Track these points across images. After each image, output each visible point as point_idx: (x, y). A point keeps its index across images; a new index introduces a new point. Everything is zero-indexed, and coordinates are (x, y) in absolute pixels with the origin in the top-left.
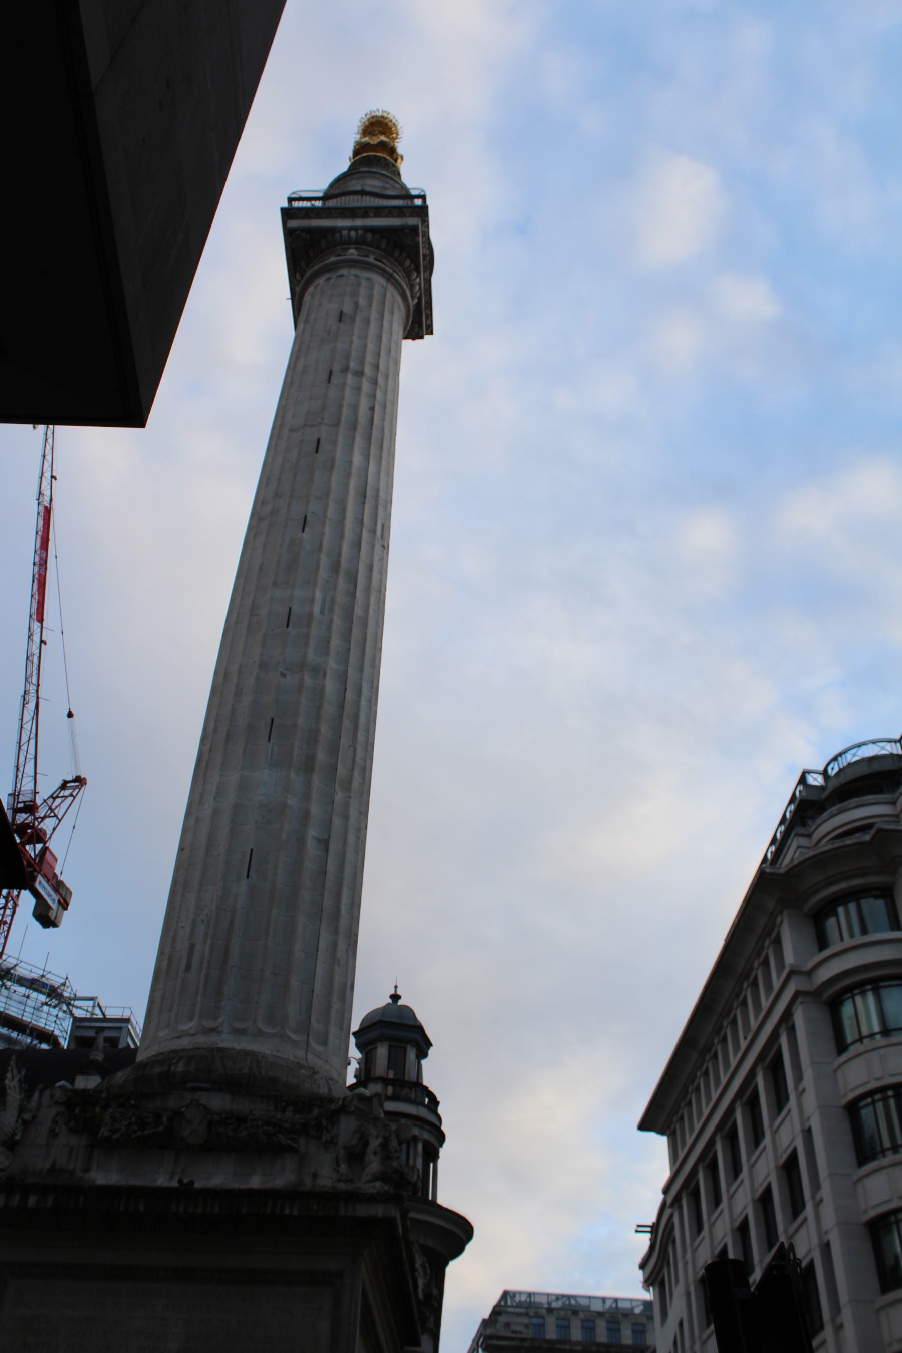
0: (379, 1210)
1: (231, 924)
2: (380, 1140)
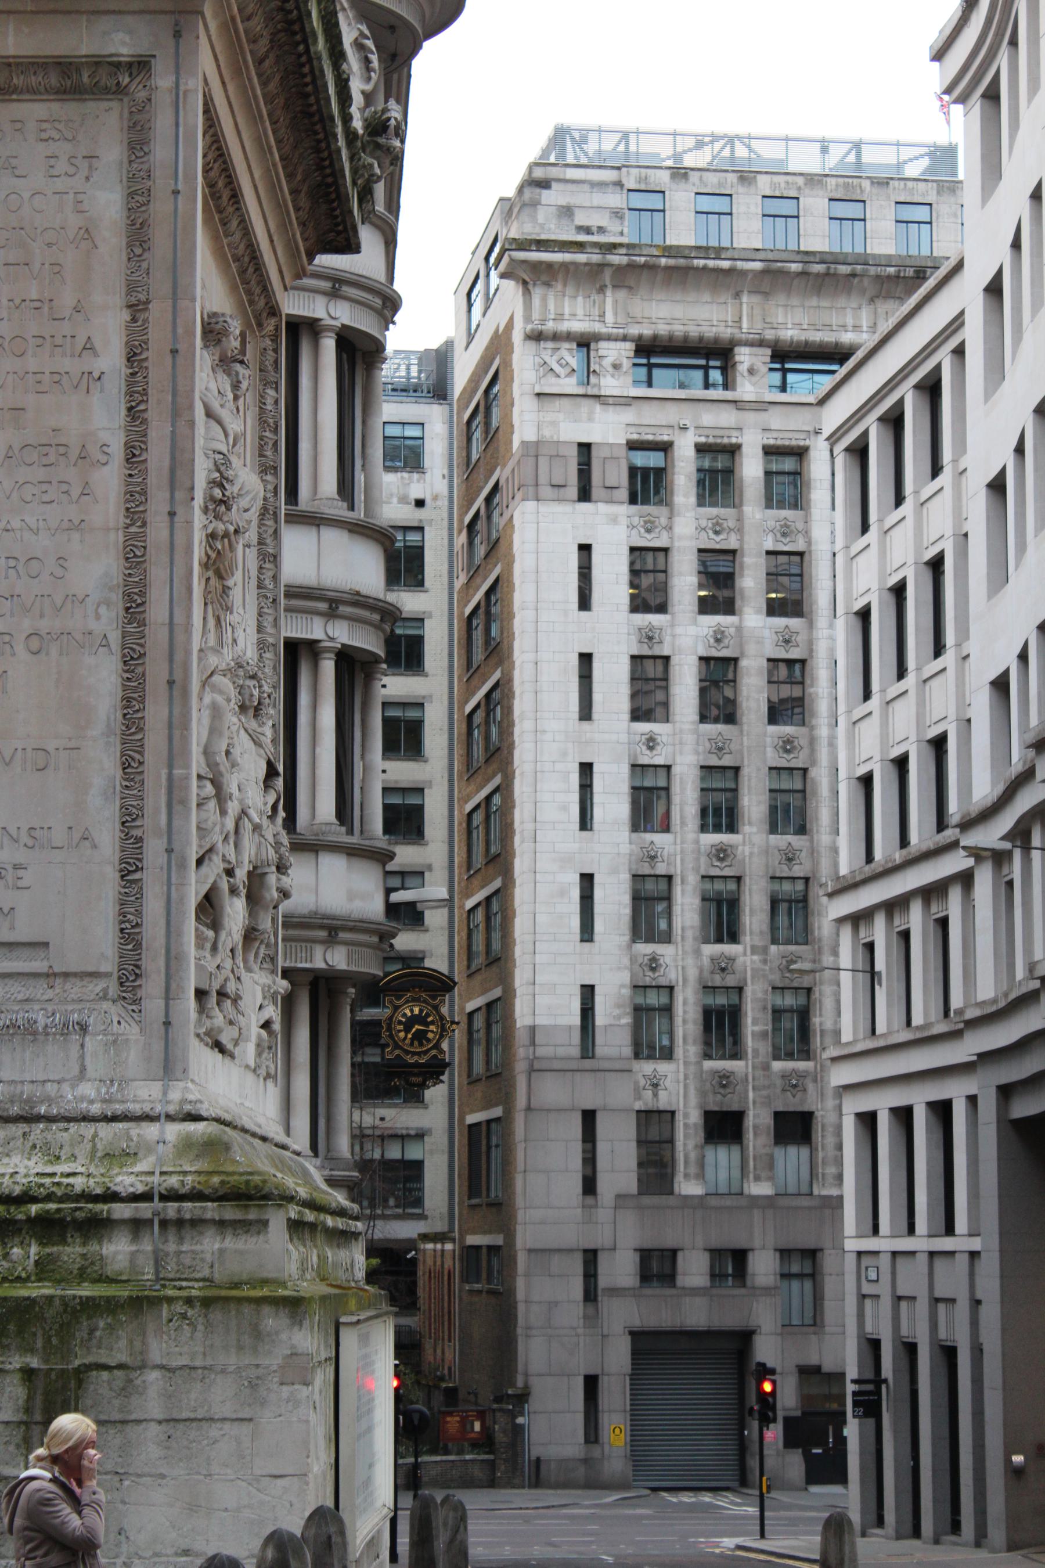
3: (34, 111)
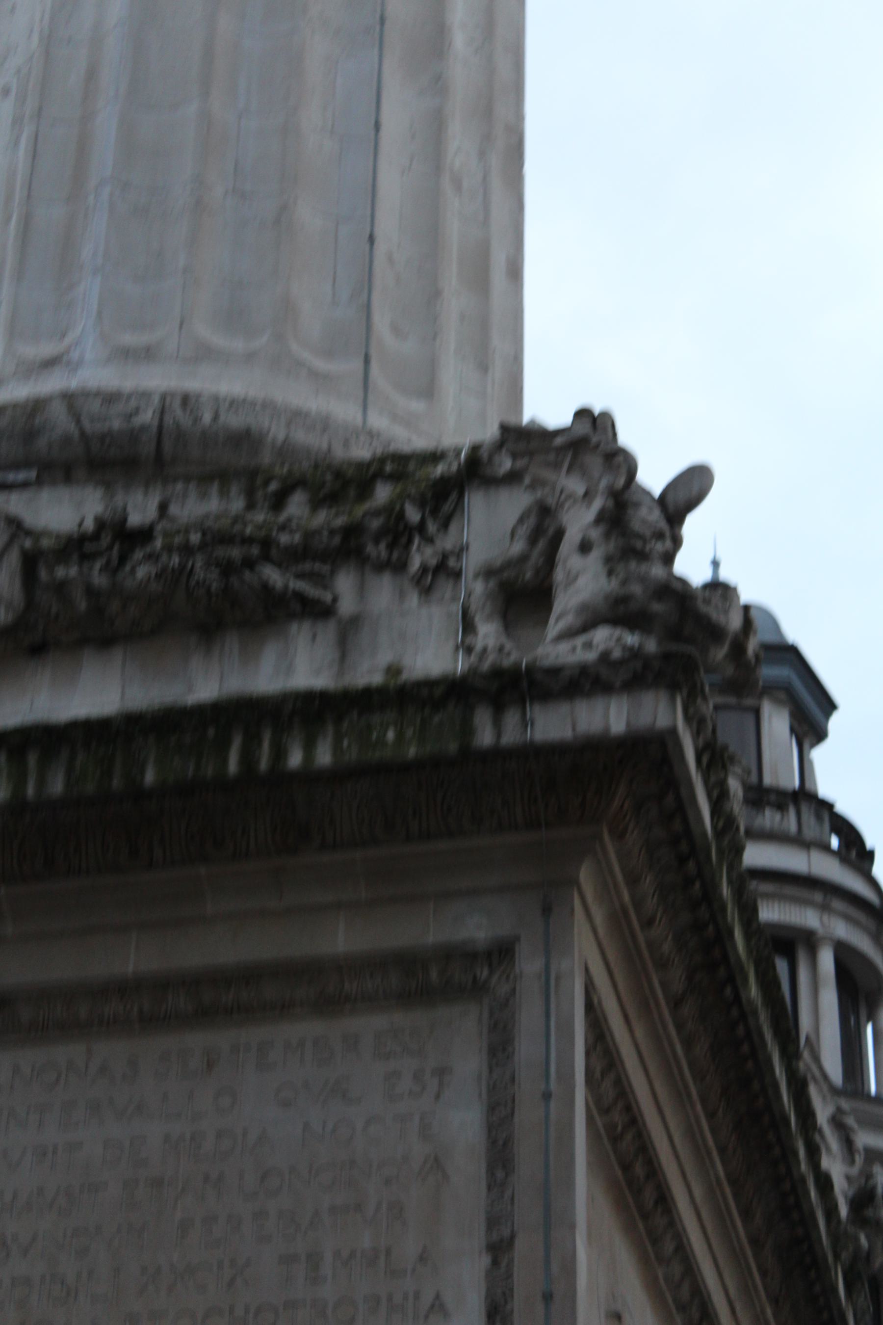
0: (612, 716)
1: (91, 74)
2: (598, 504)
3: (369, 1024)
